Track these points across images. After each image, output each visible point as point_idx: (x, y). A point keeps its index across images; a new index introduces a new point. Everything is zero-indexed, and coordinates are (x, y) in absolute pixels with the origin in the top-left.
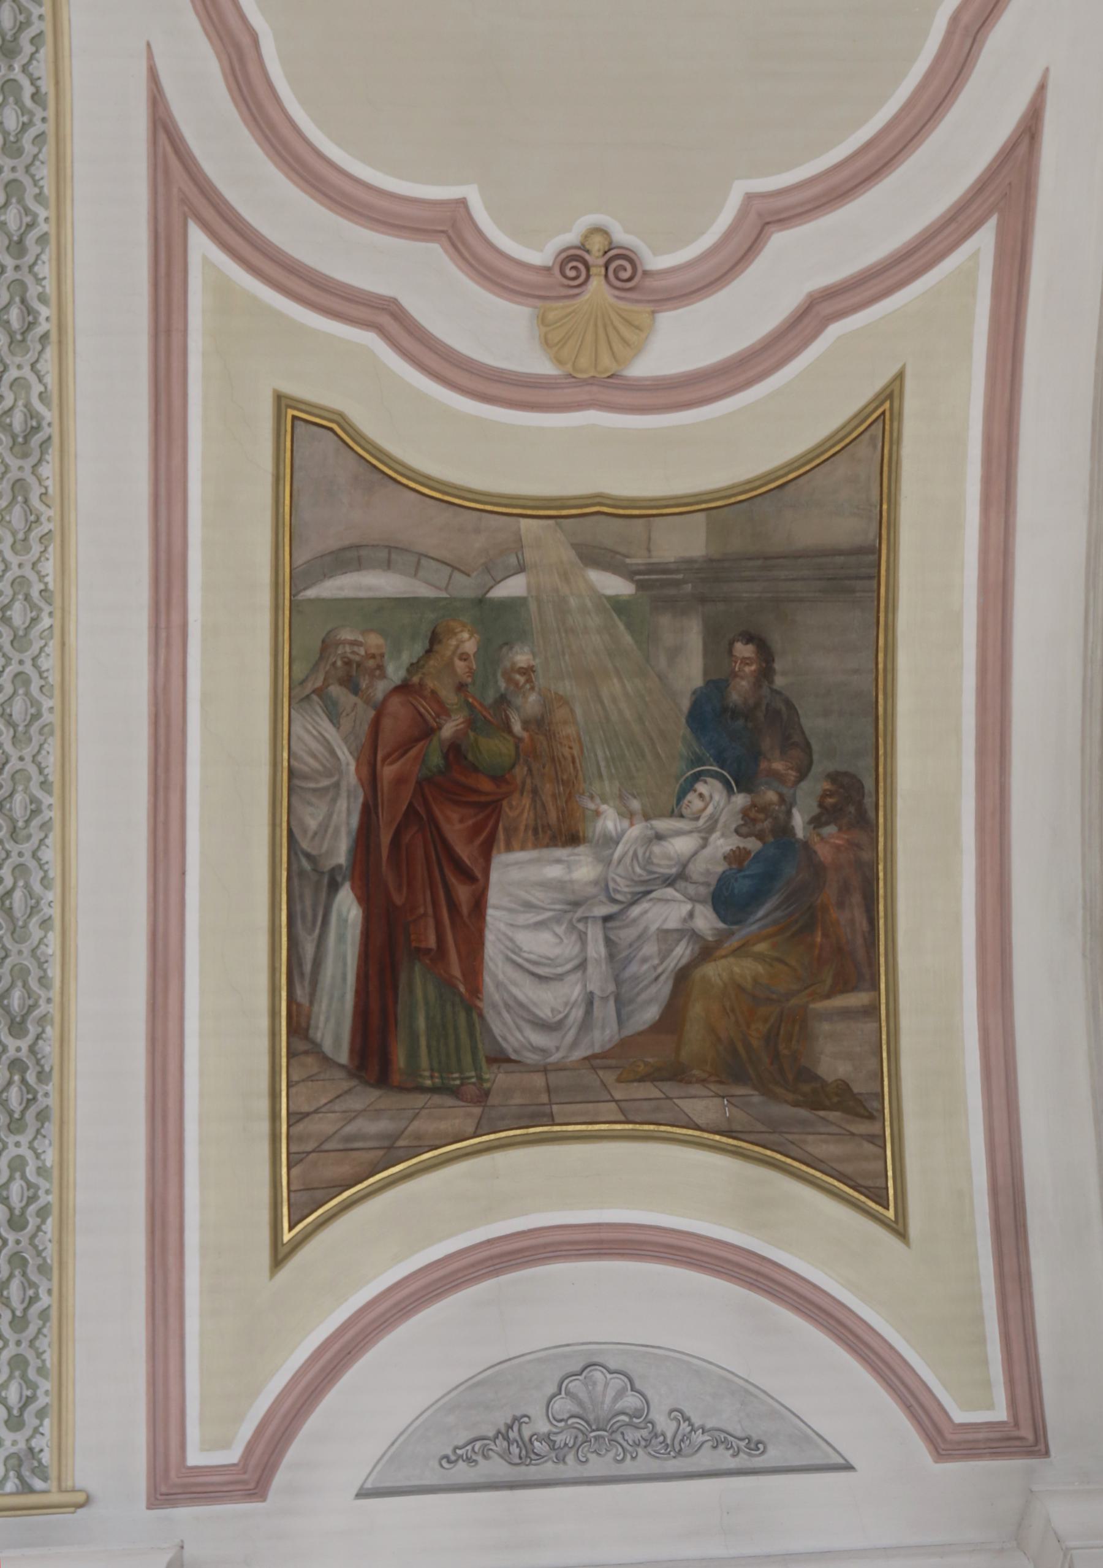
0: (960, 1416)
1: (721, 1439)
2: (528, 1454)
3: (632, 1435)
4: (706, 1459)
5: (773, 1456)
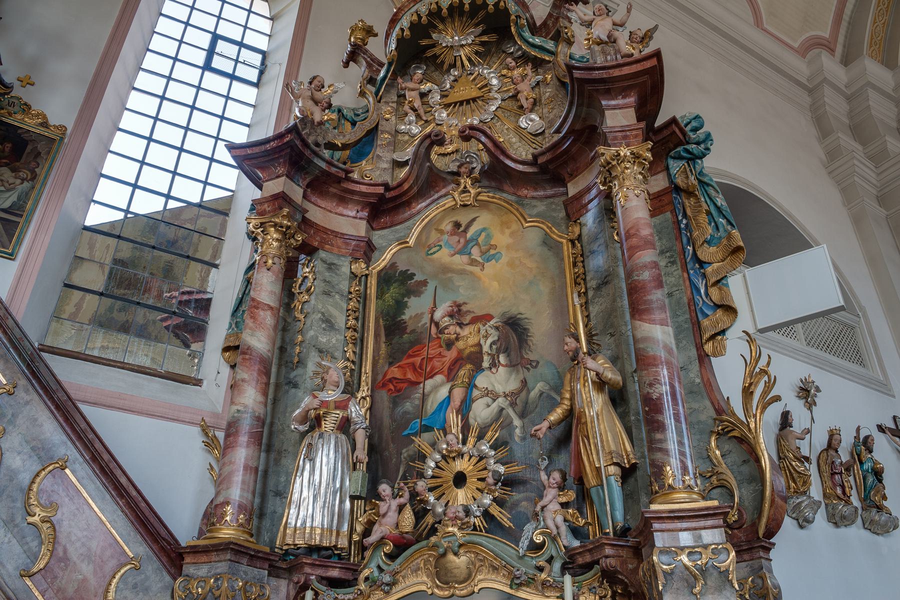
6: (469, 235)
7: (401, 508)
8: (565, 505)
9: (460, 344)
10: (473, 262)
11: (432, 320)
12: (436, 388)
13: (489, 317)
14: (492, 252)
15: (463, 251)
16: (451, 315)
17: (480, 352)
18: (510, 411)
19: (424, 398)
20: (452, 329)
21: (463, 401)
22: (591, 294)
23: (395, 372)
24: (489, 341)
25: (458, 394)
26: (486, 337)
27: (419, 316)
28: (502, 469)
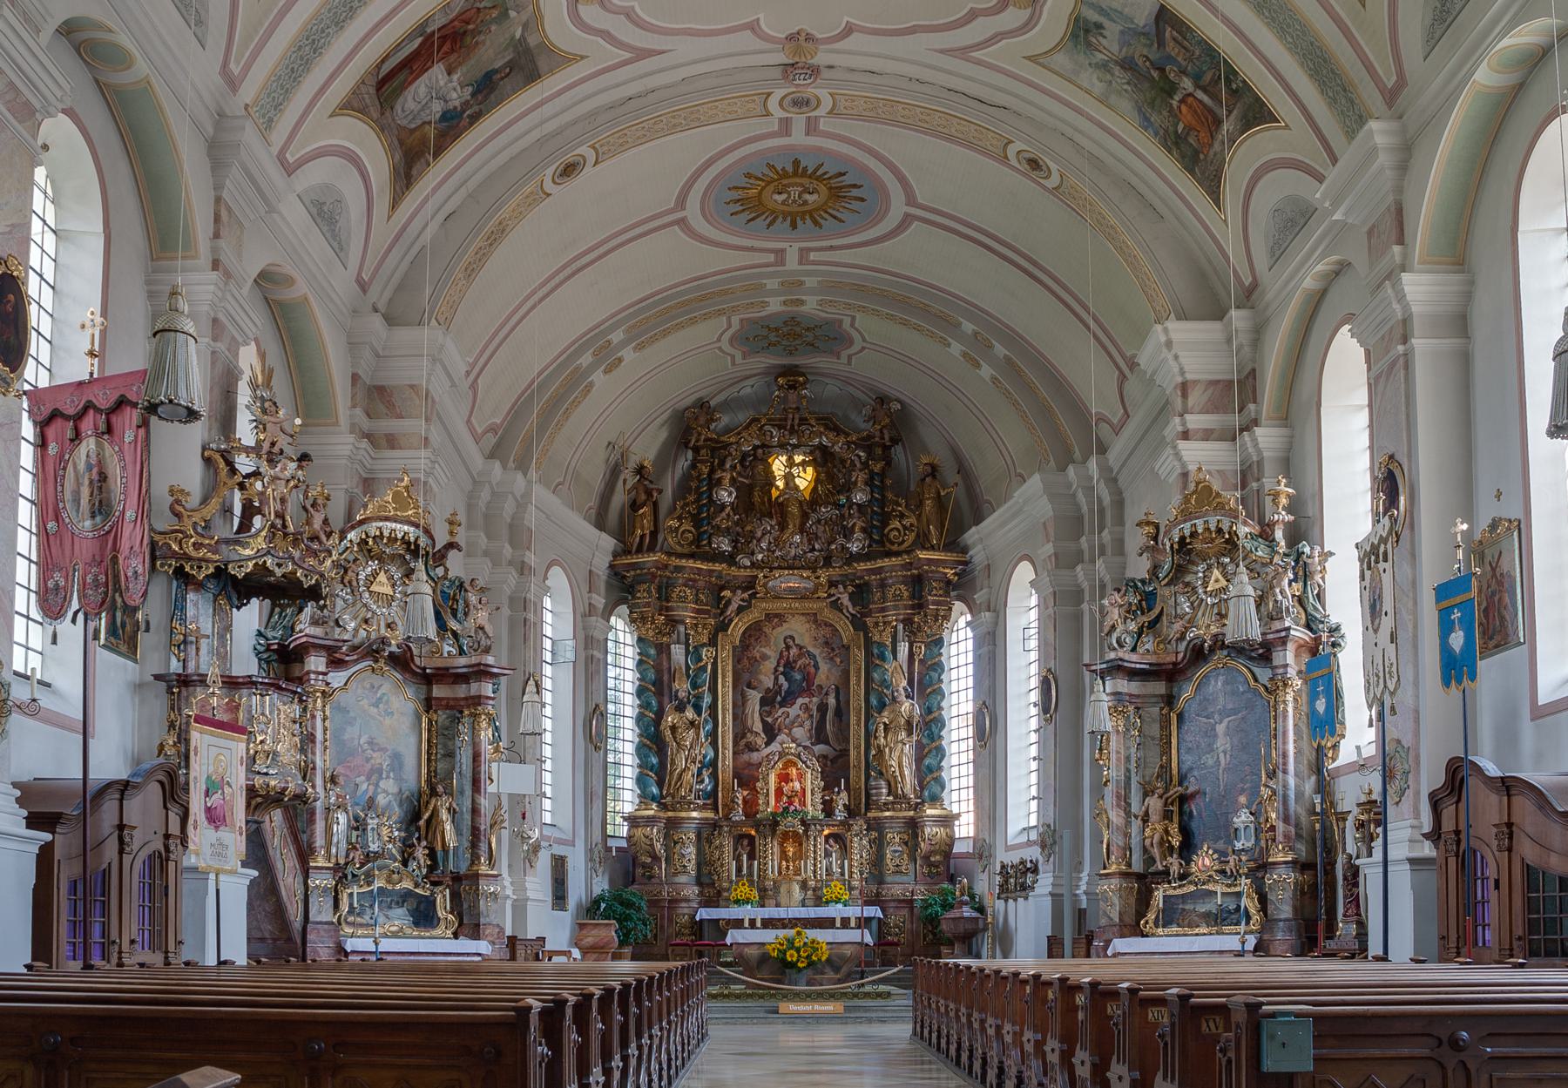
9: (373, 761)
13: (387, 750)
17: (382, 769)
26: (385, 760)
27: (353, 739)
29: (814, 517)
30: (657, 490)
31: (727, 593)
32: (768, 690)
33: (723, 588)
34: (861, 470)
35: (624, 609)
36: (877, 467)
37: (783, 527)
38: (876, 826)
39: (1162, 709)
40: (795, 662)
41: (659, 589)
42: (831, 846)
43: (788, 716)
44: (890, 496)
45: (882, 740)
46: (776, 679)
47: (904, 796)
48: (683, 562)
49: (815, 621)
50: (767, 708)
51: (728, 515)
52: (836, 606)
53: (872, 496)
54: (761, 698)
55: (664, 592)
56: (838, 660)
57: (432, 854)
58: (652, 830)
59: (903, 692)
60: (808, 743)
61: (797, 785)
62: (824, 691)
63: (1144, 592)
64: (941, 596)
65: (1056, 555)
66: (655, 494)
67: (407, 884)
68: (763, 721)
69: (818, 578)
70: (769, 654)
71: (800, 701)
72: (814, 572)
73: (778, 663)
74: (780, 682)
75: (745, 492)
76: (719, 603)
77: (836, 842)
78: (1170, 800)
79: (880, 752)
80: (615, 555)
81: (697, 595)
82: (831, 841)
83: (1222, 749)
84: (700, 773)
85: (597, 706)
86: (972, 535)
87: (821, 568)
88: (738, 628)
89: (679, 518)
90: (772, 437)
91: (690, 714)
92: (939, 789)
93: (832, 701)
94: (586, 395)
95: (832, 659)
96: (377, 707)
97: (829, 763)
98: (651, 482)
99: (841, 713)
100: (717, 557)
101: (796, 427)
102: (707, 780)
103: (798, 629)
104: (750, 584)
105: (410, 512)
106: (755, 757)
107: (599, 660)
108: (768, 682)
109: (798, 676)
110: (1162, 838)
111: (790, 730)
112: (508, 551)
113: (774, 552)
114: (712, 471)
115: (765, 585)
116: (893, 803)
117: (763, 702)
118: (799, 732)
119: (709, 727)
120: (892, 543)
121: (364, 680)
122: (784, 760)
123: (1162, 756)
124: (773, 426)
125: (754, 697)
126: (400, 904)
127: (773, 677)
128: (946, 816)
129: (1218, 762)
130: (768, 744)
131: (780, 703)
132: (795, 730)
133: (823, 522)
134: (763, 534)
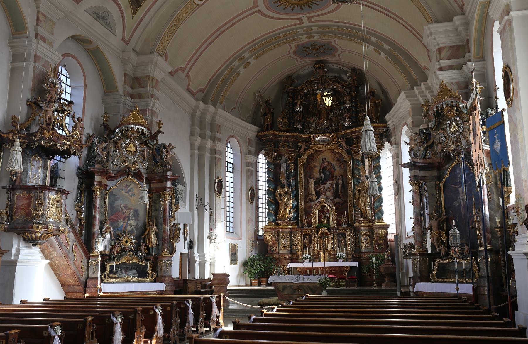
0: (125, 38)
1: (110, 27)
2: (98, 17)
3: (105, 21)
4: (108, 28)
5: (112, 31)
6: (129, 189)
7: (118, 247)
8: (145, 249)
9: (126, 214)
10: (129, 195)
11: (120, 207)
12: (121, 222)
14: (134, 194)
15: (128, 192)
16: (124, 207)
18: (134, 229)
19: (118, 224)
20: (124, 210)
21: (126, 226)
22: (153, 210)
23: (112, 217)
24: (131, 214)
25: (125, 224)
26: (131, 213)
27: (118, 206)
28: (134, 241)
29: (332, 114)
30: (272, 108)
31: (300, 144)
32: (317, 179)
33: (299, 142)
34: (347, 96)
35: (263, 152)
36: (353, 94)
37: (320, 119)
38: (356, 231)
39: (436, 182)
40: (327, 167)
41: (275, 144)
42: (340, 238)
43: (325, 188)
44: (359, 104)
45: (358, 196)
46: (320, 174)
47: (367, 217)
48: (282, 134)
49: (334, 152)
50: (316, 185)
51: (300, 115)
52: (340, 146)
53: (352, 105)
54: (314, 182)
55: (277, 144)
56: (342, 166)
57: (148, 248)
58: (272, 233)
59: (365, 177)
60: (332, 198)
61: (327, 214)
62: (338, 178)
63: (427, 133)
64: (378, 140)
65: (413, 122)
66: (272, 110)
67: (135, 261)
68: (315, 190)
69: (333, 136)
70: (317, 165)
71: (329, 182)
72: (331, 134)
73: (320, 168)
74: (321, 176)
75: (306, 107)
76: (298, 147)
77: (342, 236)
78: (441, 221)
79: (358, 201)
80: (258, 132)
81: (289, 145)
82: (340, 236)
83: (462, 198)
84: (290, 211)
85: (251, 187)
86: (387, 117)
87: (334, 133)
88: (305, 157)
89: (282, 118)
90: (315, 87)
91: (286, 189)
92: (381, 215)
93: (341, 182)
94: (238, 76)
95: (340, 166)
96: (129, 193)
97: (340, 205)
98: (270, 106)
99: (345, 186)
100: (296, 130)
101: (323, 82)
102: (293, 213)
103: (328, 156)
104: (308, 140)
105: (139, 121)
106: (313, 203)
107: (252, 170)
108: (317, 176)
109: (328, 173)
110: (438, 237)
111: (325, 193)
112: (208, 133)
113: (317, 128)
114: (294, 100)
115: (314, 140)
116: (363, 221)
117: (315, 183)
118: (328, 194)
119: (294, 193)
120: (360, 122)
121: (123, 183)
122: (321, 205)
123: (437, 202)
124: (315, 82)
125: (312, 181)
126: (134, 269)
127: (318, 174)
128: (383, 225)
129: (460, 204)
130: (317, 199)
131: (321, 183)
132: (327, 193)
133: (335, 116)
134: (313, 122)
